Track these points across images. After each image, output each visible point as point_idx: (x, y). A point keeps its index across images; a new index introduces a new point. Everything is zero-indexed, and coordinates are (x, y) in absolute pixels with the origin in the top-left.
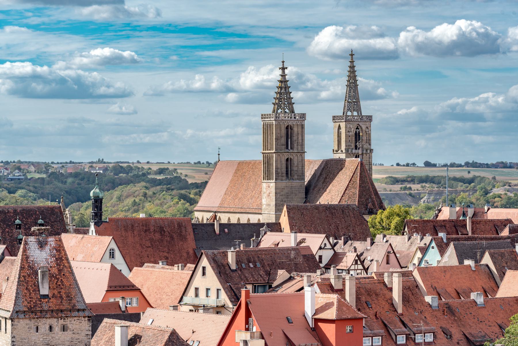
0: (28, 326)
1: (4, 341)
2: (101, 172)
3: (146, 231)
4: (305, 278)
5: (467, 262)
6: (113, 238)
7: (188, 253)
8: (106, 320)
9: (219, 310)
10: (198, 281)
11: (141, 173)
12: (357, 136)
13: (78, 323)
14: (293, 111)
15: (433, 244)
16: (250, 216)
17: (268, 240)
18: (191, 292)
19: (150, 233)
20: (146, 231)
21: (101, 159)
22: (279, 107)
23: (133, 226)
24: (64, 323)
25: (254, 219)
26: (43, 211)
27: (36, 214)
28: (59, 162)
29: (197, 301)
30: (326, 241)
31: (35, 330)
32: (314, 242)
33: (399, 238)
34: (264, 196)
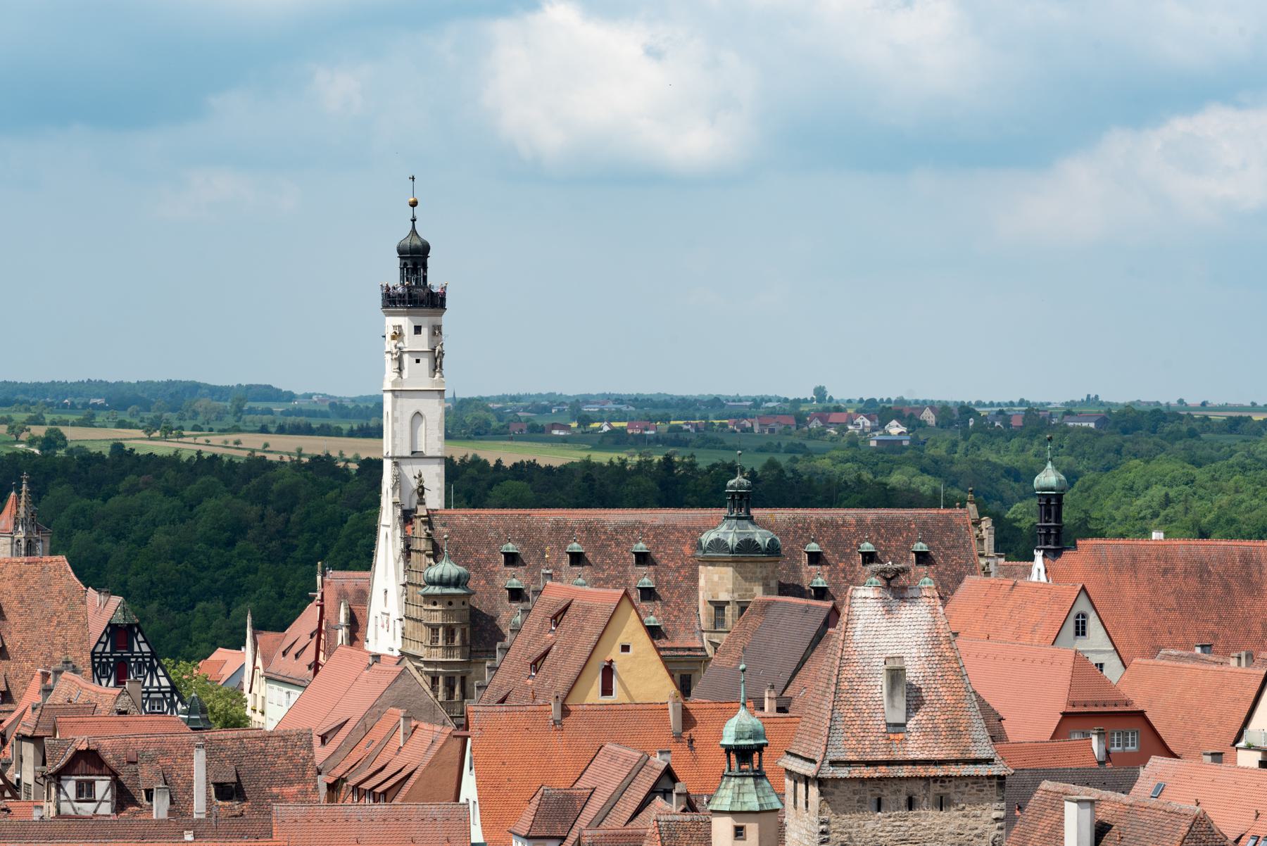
0: (857, 797)
1: (804, 832)
2: (1092, 425)
3: (1165, 572)
6: (1083, 588)
8: (1046, 785)
11: (1184, 428)
13: (974, 791)
19: (1176, 576)
20: (1165, 572)
21: (1092, 396)
23: (1134, 558)
24: (943, 791)
26: (925, 523)
27: (908, 529)
28: (996, 401)
31: (875, 805)
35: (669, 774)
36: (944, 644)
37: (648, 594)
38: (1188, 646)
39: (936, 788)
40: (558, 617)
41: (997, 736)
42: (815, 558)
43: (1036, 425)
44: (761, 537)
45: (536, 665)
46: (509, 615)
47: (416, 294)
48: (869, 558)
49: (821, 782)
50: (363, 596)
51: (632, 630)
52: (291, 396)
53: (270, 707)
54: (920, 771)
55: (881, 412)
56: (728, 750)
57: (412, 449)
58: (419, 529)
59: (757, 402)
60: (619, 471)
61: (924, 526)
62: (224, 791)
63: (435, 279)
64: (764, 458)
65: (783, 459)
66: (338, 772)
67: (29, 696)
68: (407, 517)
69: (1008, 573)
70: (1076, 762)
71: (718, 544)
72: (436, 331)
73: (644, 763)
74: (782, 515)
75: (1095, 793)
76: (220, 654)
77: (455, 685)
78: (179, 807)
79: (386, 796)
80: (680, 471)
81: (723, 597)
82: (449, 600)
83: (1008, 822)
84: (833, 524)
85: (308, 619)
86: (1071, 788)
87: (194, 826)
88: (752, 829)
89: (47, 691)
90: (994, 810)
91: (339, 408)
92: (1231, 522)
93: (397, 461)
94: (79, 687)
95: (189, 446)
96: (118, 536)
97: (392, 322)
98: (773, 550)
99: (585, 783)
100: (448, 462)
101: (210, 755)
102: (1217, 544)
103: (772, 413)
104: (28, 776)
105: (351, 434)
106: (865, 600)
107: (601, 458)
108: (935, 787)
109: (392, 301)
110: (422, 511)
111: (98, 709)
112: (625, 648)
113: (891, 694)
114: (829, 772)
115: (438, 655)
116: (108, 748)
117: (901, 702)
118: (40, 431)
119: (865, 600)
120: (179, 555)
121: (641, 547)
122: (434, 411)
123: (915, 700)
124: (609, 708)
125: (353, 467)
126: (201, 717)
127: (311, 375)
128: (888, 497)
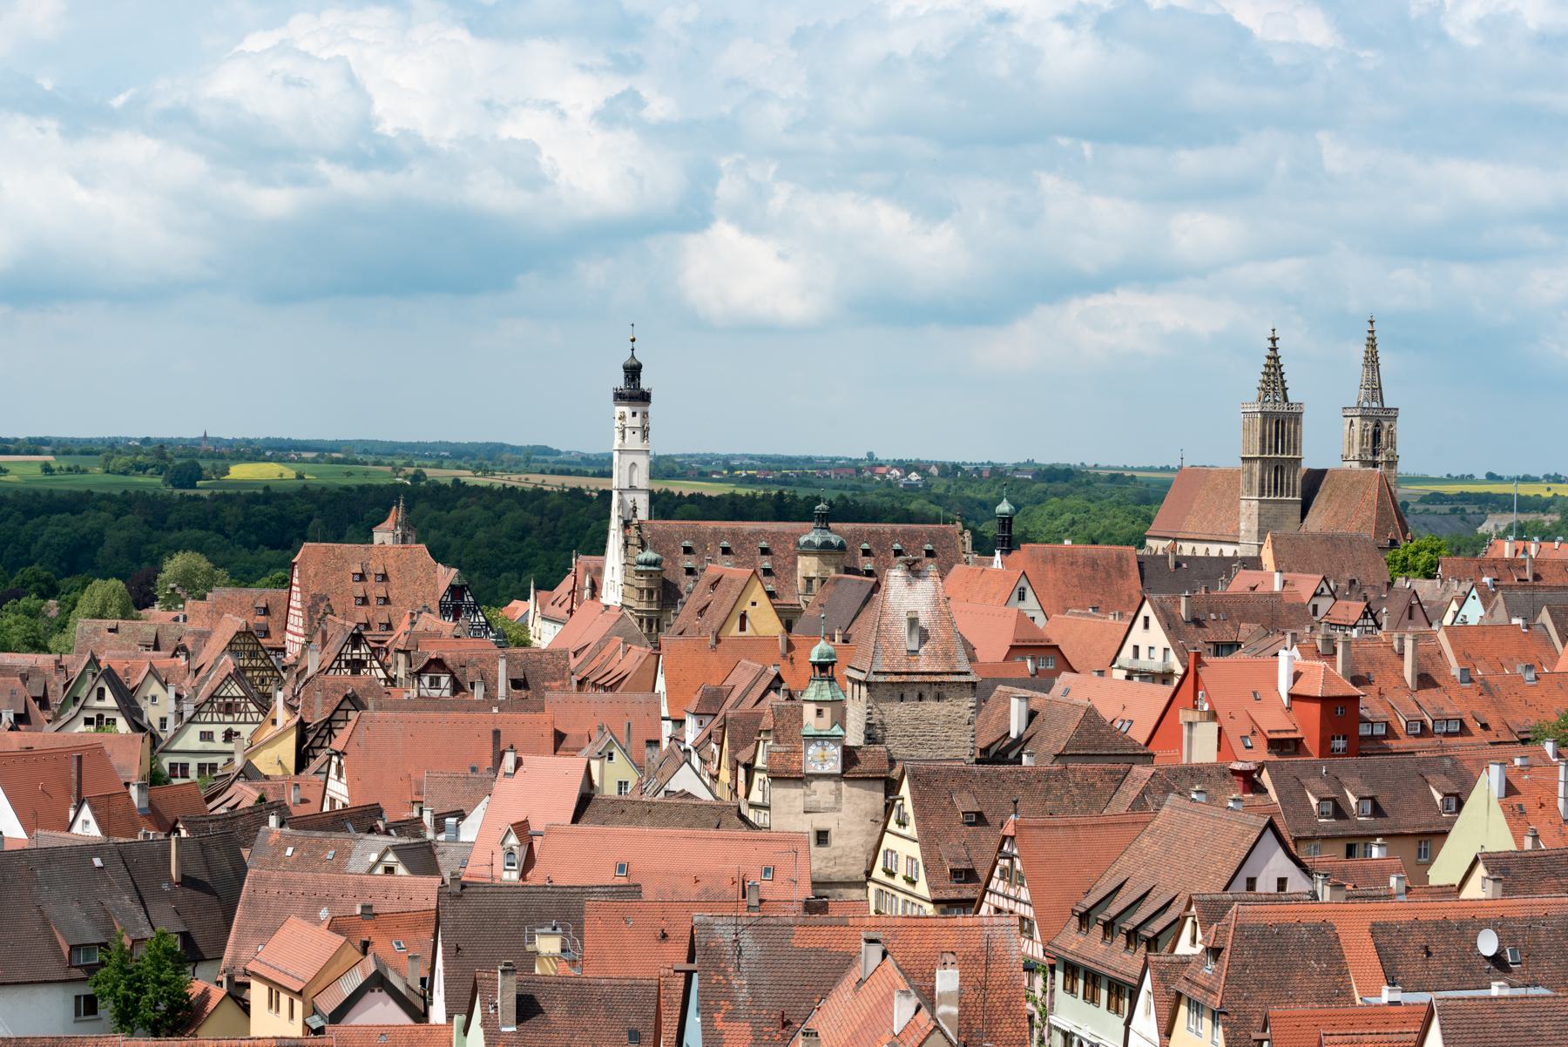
4: (1289, 637)
5: (1515, 621)
7: (1130, 596)
8: (1000, 687)
9: (1165, 677)
10: (1137, 635)
12: (1376, 436)
14: (1286, 400)
15: (1474, 592)
16: (1224, 547)
17: (1241, 582)
18: (1127, 652)
22: (1267, 394)
25: (1228, 551)
29: (1137, 665)
30: (1324, 585)
32: (1306, 585)
33: (1428, 582)
34: (1243, 518)
35: (778, 678)
36: (942, 604)
37: (767, 572)
38: (1084, 608)
39: (935, 688)
40: (715, 584)
41: (972, 659)
42: (866, 553)
43: (997, 472)
44: (834, 539)
45: (701, 612)
46: (685, 583)
47: (634, 393)
48: (898, 553)
49: (868, 684)
50: (599, 571)
51: (758, 593)
52: (558, 453)
53: (544, 635)
54: (927, 678)
55: (907, 467)
56: (814, 664)
57: (630, 485)
58: (633, 532)
59: (833, 460)
60: (752, 500)
61: (931, 535)
62: (517, 684)
63: (645, 383)
64: (838, 492)
65: (848, 494)
66: (584, 674)
67: (403, 626)
68: (626, 525)
69: (980, 563)
70: (1017, 675)
71: (809, 544)
72: (645, 415)
73: (763, 672)
74: (847, 527)
75: (1029, 693)
76: (515, 603)
77: (653, 624)
78: (490, 693)
79: (612, 688)
80: (787, 500)
81: (812, 574)
82: (650, 573)
83: (977, 709)
84: (877, 533)
85: (567, 584)
86: (1015, 690)
87: (499, 705)
88: (827, 711)
89: (413, 623)
90: (969, 702)
91: (586, 460)
92: (1110, 535)
93: (621, 492)
94: (432, 622)
95: (498, 481)
96: (456, 533)
97: (619, 409)
98: (842, 547)
99: (729, 682)
100: (651, 493)
101: (508, 662)
102: (1103, 548)
103: (842, 467)
104: (401, 672)
105: (594, 475)
106: (895, 577)
107: (742, 491)
108: (935, 688)
109: (620, 397)
110: (635, 521)
111: (443, 634)
112: (754, 604)
113: (910, 633)
114: (873, 678)
115: (643, 606)
116: (449, 658)
117: (916, 638)
118: (411, 471)
119: (895, 577)
120: (492, 545)
121: (764, 544)
122: (643, 463)
123: (924, 637)
124: (744, 639)
125: (595, 494)
126: (504, 640)
127: (571, 440)
128: (909, 518)
